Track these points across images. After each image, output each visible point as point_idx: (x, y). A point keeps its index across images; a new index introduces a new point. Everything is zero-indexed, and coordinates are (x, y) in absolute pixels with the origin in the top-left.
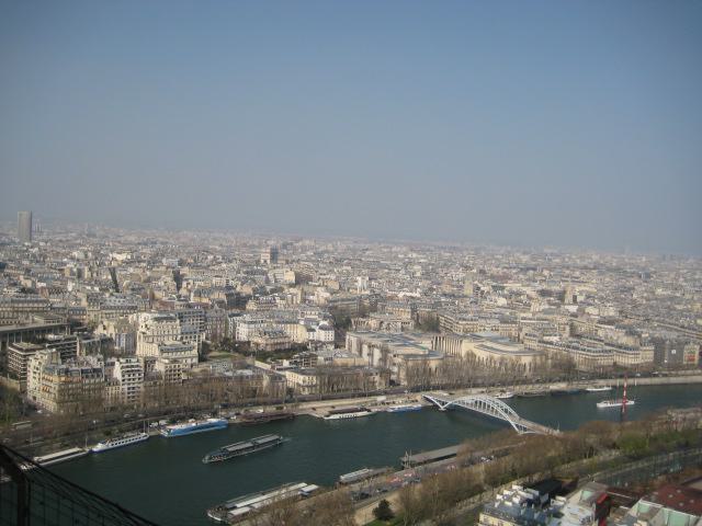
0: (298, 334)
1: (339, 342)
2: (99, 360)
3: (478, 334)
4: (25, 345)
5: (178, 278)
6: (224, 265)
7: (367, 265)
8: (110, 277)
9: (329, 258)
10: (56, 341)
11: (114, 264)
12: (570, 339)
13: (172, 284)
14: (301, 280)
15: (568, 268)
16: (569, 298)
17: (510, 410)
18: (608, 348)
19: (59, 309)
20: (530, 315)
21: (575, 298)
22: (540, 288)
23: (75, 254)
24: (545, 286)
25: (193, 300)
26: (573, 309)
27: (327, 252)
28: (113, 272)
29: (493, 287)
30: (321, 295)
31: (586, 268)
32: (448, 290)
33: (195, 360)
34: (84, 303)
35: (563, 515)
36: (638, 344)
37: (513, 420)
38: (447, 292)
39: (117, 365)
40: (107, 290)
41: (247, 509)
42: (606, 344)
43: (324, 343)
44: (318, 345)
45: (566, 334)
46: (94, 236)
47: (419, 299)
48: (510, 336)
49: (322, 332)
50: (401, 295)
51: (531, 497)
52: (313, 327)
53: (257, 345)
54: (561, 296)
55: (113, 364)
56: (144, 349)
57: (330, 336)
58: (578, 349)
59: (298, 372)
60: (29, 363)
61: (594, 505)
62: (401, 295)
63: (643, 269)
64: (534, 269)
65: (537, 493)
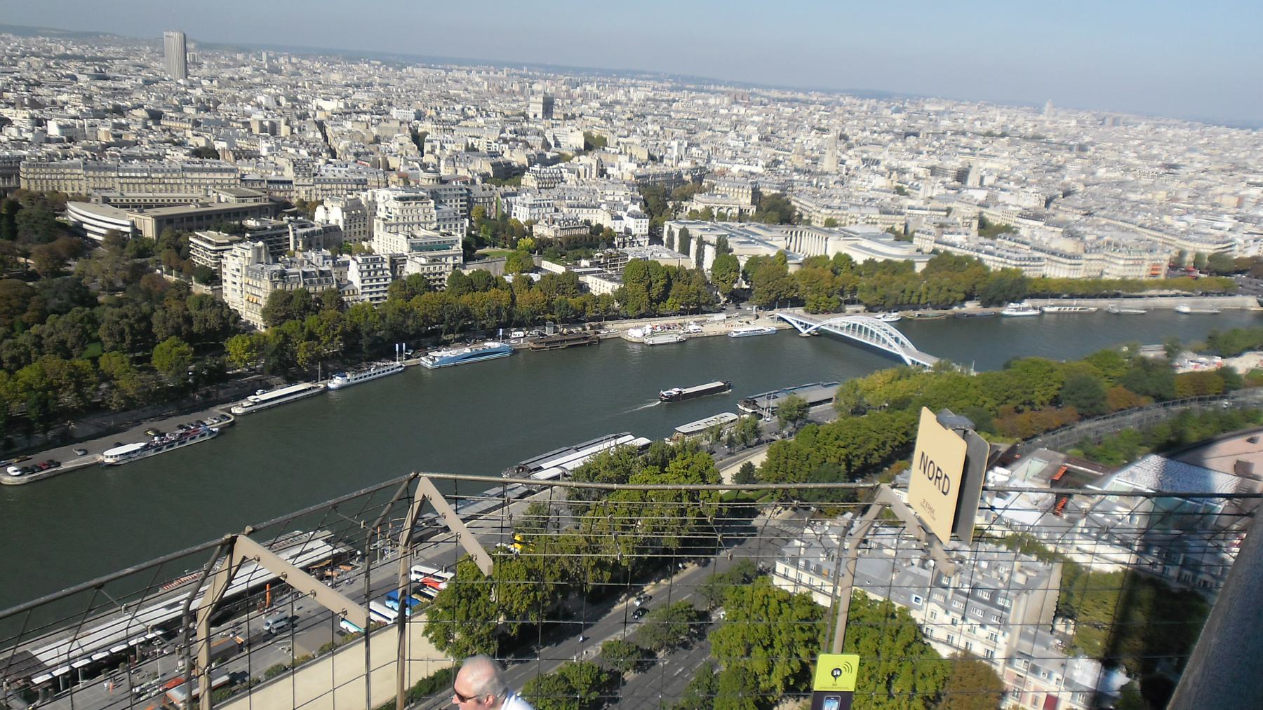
2: (325, 258)
3: (847, 228)
5: (418, 139)
6: (481, 121)
9: (624, 112)
12: (982, 239)
13: (412, 148)
14: (591, 145)
15: (964, 134)
16: (972, 180)
17: (902, 338)
18: (1037, 254)
19: (253, 181)
20: (921, 204)
21: (982, 179)
22: (930, 164)
23: (261, 99)
24: (935, 161)
25: (445, 171)
26: (981, 195)
27: (617, 102)
29: (864, 160)
31: (989, 134)
32: (800, 164)
36: (1080, 251)
37: (909, 353)
38: (799, 166)
39: (353, 263)
46: (279, 72)
48: (891, 230)
49: (632, 220)
50: (735, 169)
52: (619, 213)
54: (962, 176)
55: (346, 264)
56: (385, 243)
59: (604, 278)
60: (223, 261)
62: (735, 169)
63: (1075, 138)
64: (916, 135)
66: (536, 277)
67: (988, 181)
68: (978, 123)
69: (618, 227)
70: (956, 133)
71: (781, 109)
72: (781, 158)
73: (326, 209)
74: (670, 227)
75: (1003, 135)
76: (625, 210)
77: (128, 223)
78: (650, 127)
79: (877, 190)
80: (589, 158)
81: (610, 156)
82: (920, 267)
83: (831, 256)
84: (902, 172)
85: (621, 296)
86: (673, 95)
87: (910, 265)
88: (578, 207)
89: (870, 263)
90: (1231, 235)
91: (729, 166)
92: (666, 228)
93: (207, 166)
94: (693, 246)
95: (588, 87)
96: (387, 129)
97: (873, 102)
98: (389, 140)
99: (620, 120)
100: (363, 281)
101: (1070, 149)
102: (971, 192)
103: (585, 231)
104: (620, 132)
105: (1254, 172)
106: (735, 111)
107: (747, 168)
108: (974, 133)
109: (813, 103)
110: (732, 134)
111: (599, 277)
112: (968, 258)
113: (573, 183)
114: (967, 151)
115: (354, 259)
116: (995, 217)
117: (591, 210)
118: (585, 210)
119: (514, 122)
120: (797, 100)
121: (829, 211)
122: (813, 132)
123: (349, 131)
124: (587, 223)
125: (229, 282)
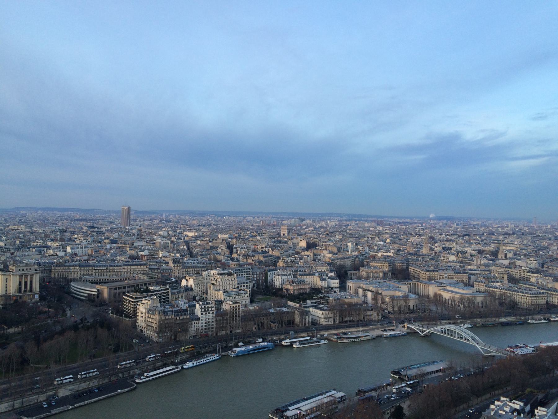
0: (316, 281)
1: (343, 287)
3: (439, 281)
4: (134, 295)
5: (230, 247)
6: (259, 238)
7: (352, 235)
8: (185, 247)
10: (155, 291)
11: (187, 238)
12: (510, 284)
13: (227, 251)
14: (311, 246)
15: (493, 234)
19: (154, 269)
20: (475, 268)
21: (506, 255)
22: (477, 248)
23: (161, 233)
24: (480, 247)
25: (242, 261)
26: (506, 262)
28: (187, 243)
29: (443, 248)
32: (412, 251)
33: (248, 301)
34: (171, 265)
38: (411, 252)
39: (197, 305)
40: (185, 256)
42: (538, 288)
43: (332, 288)
45: (506, 281)
46: (170, 222)
47: (392, 257)
48: (463, 282)
50: (380, 255)
52: (324, 277)
53: (288, 290)
54: (495, 254)
55: (195, 306)
57: (335, 283)
58: (518, 292)
59: (318, 309)
60: (138, 306)
62: (380, 255)
64: (469, 235)
67: (510, 255)
68: (500, 229)
70: (489, 234)
71: (400, 226)
72: (401, 249)
73: (187, 280)
76: (327, 276)
77: (96, 290)
78: (337, 237)
79: (452, 262)
80: (309, 252)
81: (319, 251)
84: (464, 253)
86: (348, 223)
88: (304, 275)
91: (376, 253)
93: (134, 263)
95: (308, 221)
98: (216, 248)
99: (323, 235)
100: (202, 314)
101: (550, 239)
102: (501, 261)
104: (322, 240)
106: (378, 228)
107: (385, 254)
108: (498, 234)
109: (416, 223)
111: (315, 308)
113: (302, 264)
114: (496, 242)
116: (516, 273)
117: (310, 277)
118: (308, 277)
120: (407, 223)
121: (428, 273)
122: (416, 236)
123: (199, 245)
125: (140, 316)
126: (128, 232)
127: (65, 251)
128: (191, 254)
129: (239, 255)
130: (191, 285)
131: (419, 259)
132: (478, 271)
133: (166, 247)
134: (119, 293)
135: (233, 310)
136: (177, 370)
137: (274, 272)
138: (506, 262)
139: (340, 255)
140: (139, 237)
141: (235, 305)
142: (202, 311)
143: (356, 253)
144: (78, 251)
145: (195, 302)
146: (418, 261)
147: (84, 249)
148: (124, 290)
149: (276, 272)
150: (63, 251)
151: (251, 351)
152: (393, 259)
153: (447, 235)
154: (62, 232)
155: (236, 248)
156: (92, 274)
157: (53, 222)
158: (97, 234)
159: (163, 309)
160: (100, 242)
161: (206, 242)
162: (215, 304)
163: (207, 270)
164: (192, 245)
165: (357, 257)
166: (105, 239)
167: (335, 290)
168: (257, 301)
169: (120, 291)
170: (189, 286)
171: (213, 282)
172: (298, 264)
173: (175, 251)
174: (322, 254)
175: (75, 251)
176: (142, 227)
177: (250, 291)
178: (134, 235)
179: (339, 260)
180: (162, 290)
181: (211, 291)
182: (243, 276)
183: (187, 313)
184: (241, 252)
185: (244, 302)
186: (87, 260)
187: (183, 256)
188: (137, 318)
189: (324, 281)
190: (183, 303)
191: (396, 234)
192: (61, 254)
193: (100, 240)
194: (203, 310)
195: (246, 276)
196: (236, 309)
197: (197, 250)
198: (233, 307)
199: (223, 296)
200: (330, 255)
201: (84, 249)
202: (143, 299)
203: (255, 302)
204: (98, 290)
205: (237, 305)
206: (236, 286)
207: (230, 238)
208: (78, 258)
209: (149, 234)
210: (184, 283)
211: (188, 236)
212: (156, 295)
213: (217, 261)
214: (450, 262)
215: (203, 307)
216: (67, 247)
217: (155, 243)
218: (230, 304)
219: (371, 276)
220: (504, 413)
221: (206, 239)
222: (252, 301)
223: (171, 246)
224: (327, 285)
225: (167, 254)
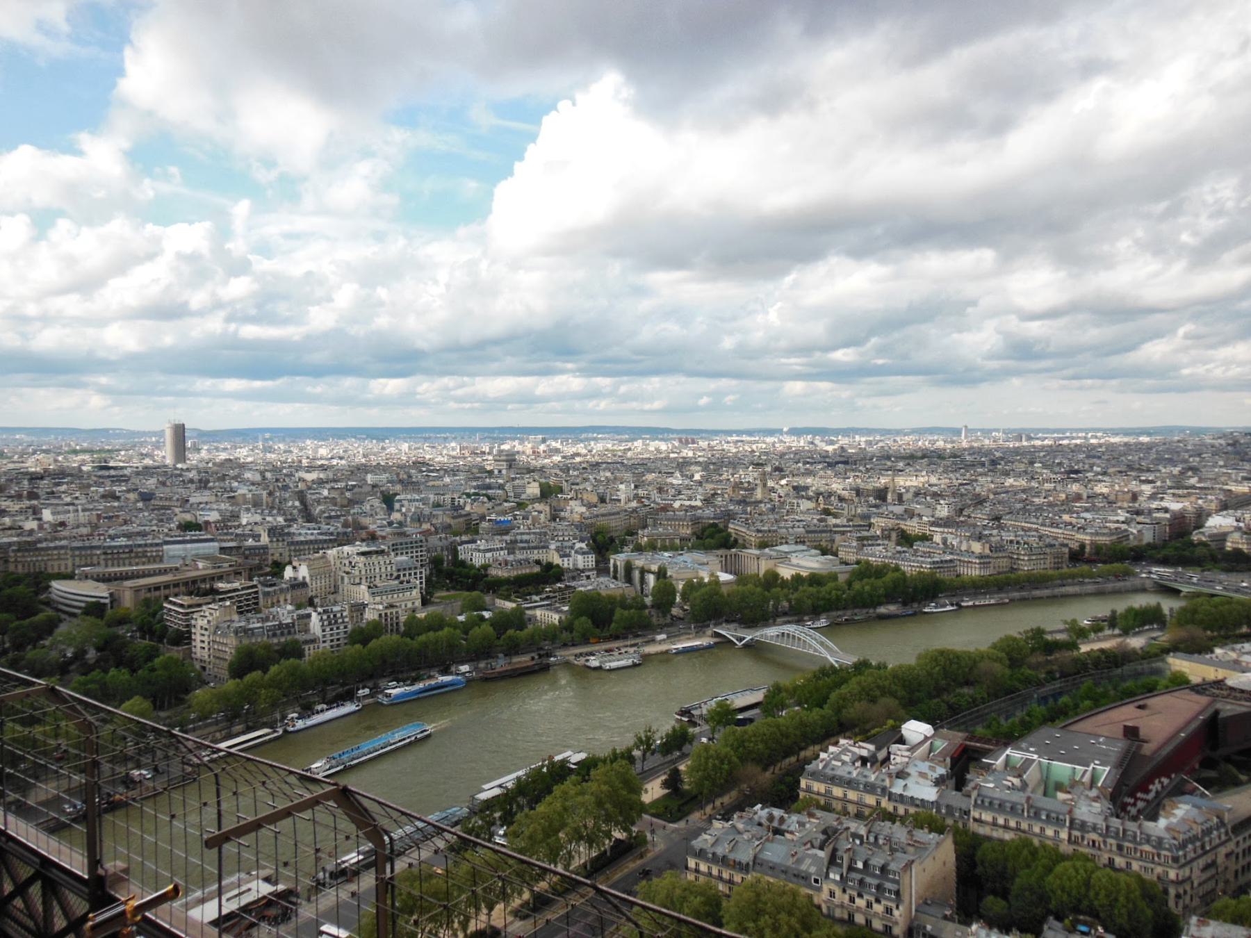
4: (186, 600)
8: (297, 503)
10: (229, 591)
11: (301, 486)
12: (899, 548)
14: (547, 493)
21: (900, 496)
26: (899, 509)
28: (301, 496)
30: (576, 510)
33: (418, 603)
34: (265, 539)
35: (909, 774)
36: (987, 551)
39: (314, 615)
40: (294, 520)
41: (497, 791)
43: (583, 571)
44: (577, 573)
47: (700, 508)
49: (580, 557)
50: (677, 505)
51: (864, 753)
55: (309, 616)
57: (591, 560)
59: (551, 610)
61: (948, 760)
65: (872, 747)
66: (487, 614)
69: (566, 563)
72: (719, 492)
73: (294, 568)
74: (615, 560)
75: (923, 457)
77: (107, 595)
78: (602, 473)
82: (842, 578)
83: (761, 575)
85: (567, 627)
87: (833, 577)
89: (797, 579)
90: (1124, 527)
92: (612, 561)
93: (188, 538)
94: (636, 574)
96: (360, 493)
97: (809, 437)
98: (360, 502)
100: (324, 631)
101: (983, 465)
102: (891, 508)
103: (537, 569)
105: (1149, 470)
107: (687, 503)
108: (896, 457)
110: (678, 474)
112: (885, 566)
115: (315, 611)
116: (912, 526)
118: (536, 551)
119: (477, 479)
121: (760, 535)
122: (751, 468)
123: (325, 498)
124: (538, 562)
125: (198, 641)
126: (180, 475)
127: (40, 519)
128: (309, 518)
129: (405, 515)
130: (304, 578)
131: (749, 509)
132: (849, 526)
133: (257, 503)
134: (157, 599)
135: (386, 620)
136: (276, 735)
137: (470, 546)
138: (899, 509)
139: (602, 509)
140: (203, 484)
141: (388, 612)
142: (323, 625)
143: (634, 504)
144: (70, 518)
145: (309, 610)
146: (746, 514)
147: (81, 514)
148: (167, 592)
149: (474, 546)
150: (34, 519)
151: (420, 693)
152: (700, 511)
153: (808, 463)
154: (32, 479)
155: (400, 501)
156: (99, 563)
157: (16, 457)
158: (112, 481)
159: (243, 624)
160: (118, 498)
161: (339, 492)
162: (351, 611)
163: (339, 546)
164: (310, 497)
165: (635, 510)
166: (128, 491)
167: (587, 574)
168: (438, 600)
169: (157, 593)
170: (301, 578)
171: (348, 569)
172: (519, 528)
173: (275, 512)
174: (568, 508)
175: (61, 518)
176: (210, 465)
177: (421, 583)
178: (191, 481)
179: (601, 518)
180: (243, 589)
181: (346, 587)
182: (410, 555)
183: (292, 630)
184: (409, 510)
185: (410, 605)
186: (87, 535)
187: (291, 520)
188: (194, 644)
189: (566, 559)
190: (286, 612)
191: (714, 464)
192: (31, 525)
193: (118, 494)
194: (326, 623)
195: (415, 554)
196: (392, 619)
197: (320, 507)
198: (386, 614)
199: (367, 595)
200: (583, 509)
201: (81, 514)
202: (204, 608)
203: (433, 603)
204: (111, 595)
205: (394, 611)
206: (395, 574)
207: (389, 482)
208: (65, 533)
209: (223, 478)
210: (288, 573)
211: (304, 480)
212: (230, 598)
213: (359, 527)
214: (802, 512)
215: (325, 617)
216: (44, 511)
217: (233, 497)
218: (378, 610)
219: (659, 545)
220: (839, 764)
221: (339, 485)
222: (425, 602)
223: (267, 503)
224: (574, 565)
225: (258, 518)
